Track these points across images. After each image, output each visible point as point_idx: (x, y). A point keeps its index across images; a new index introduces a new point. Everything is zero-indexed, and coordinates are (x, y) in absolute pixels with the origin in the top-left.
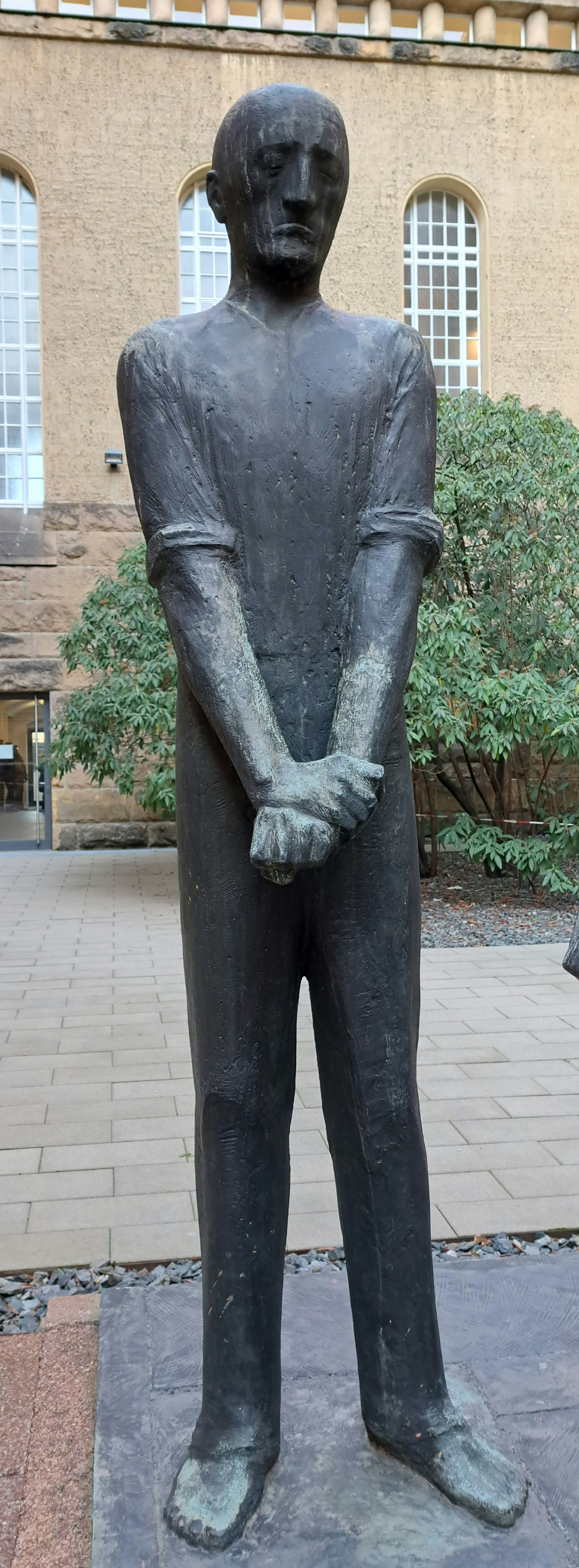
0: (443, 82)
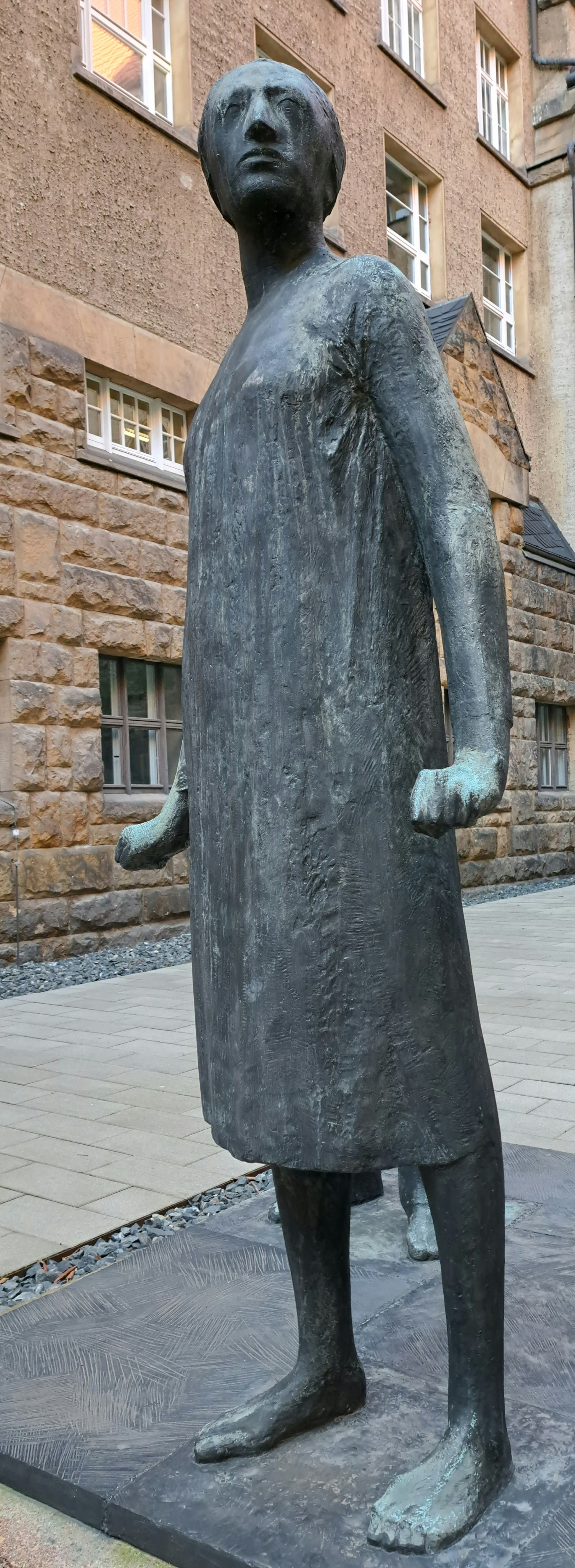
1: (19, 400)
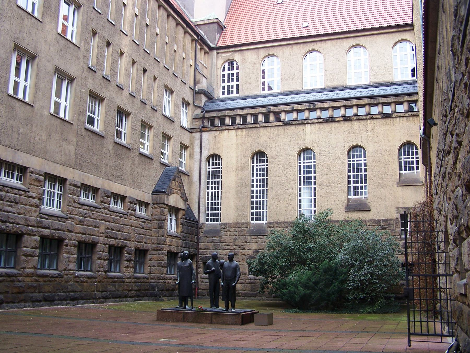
0: (355, 124)
1: (102, 202)
